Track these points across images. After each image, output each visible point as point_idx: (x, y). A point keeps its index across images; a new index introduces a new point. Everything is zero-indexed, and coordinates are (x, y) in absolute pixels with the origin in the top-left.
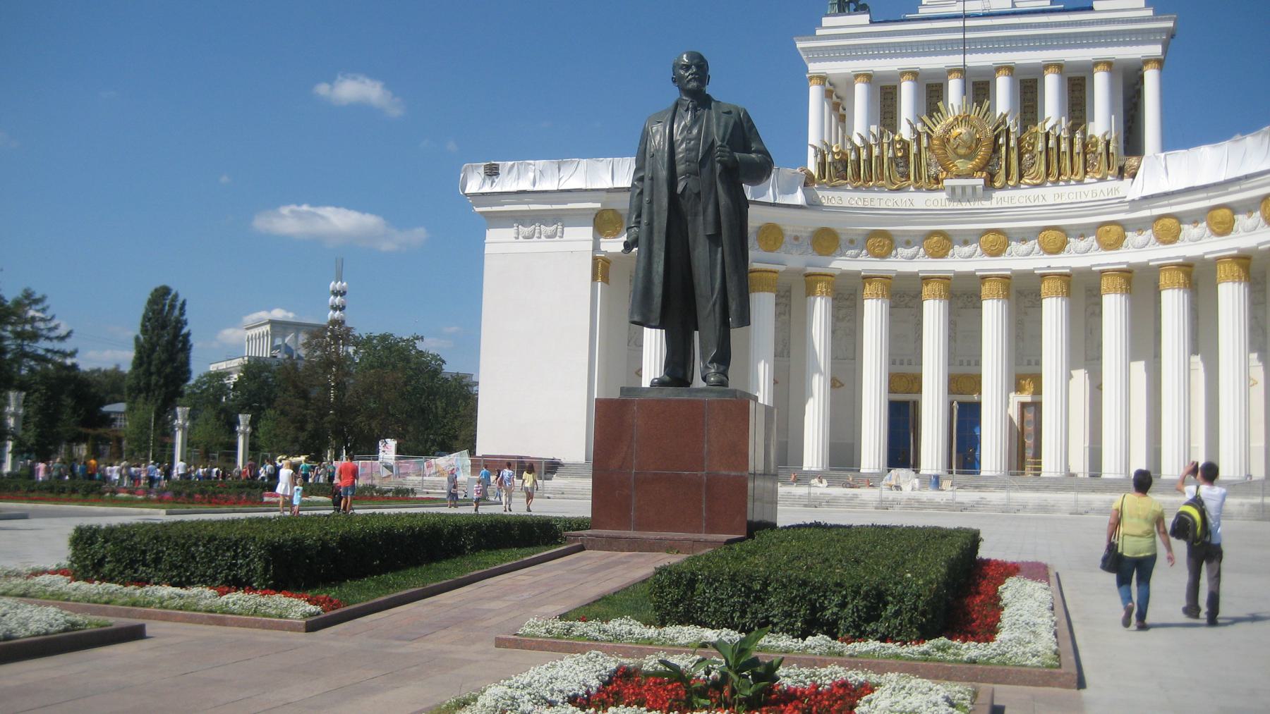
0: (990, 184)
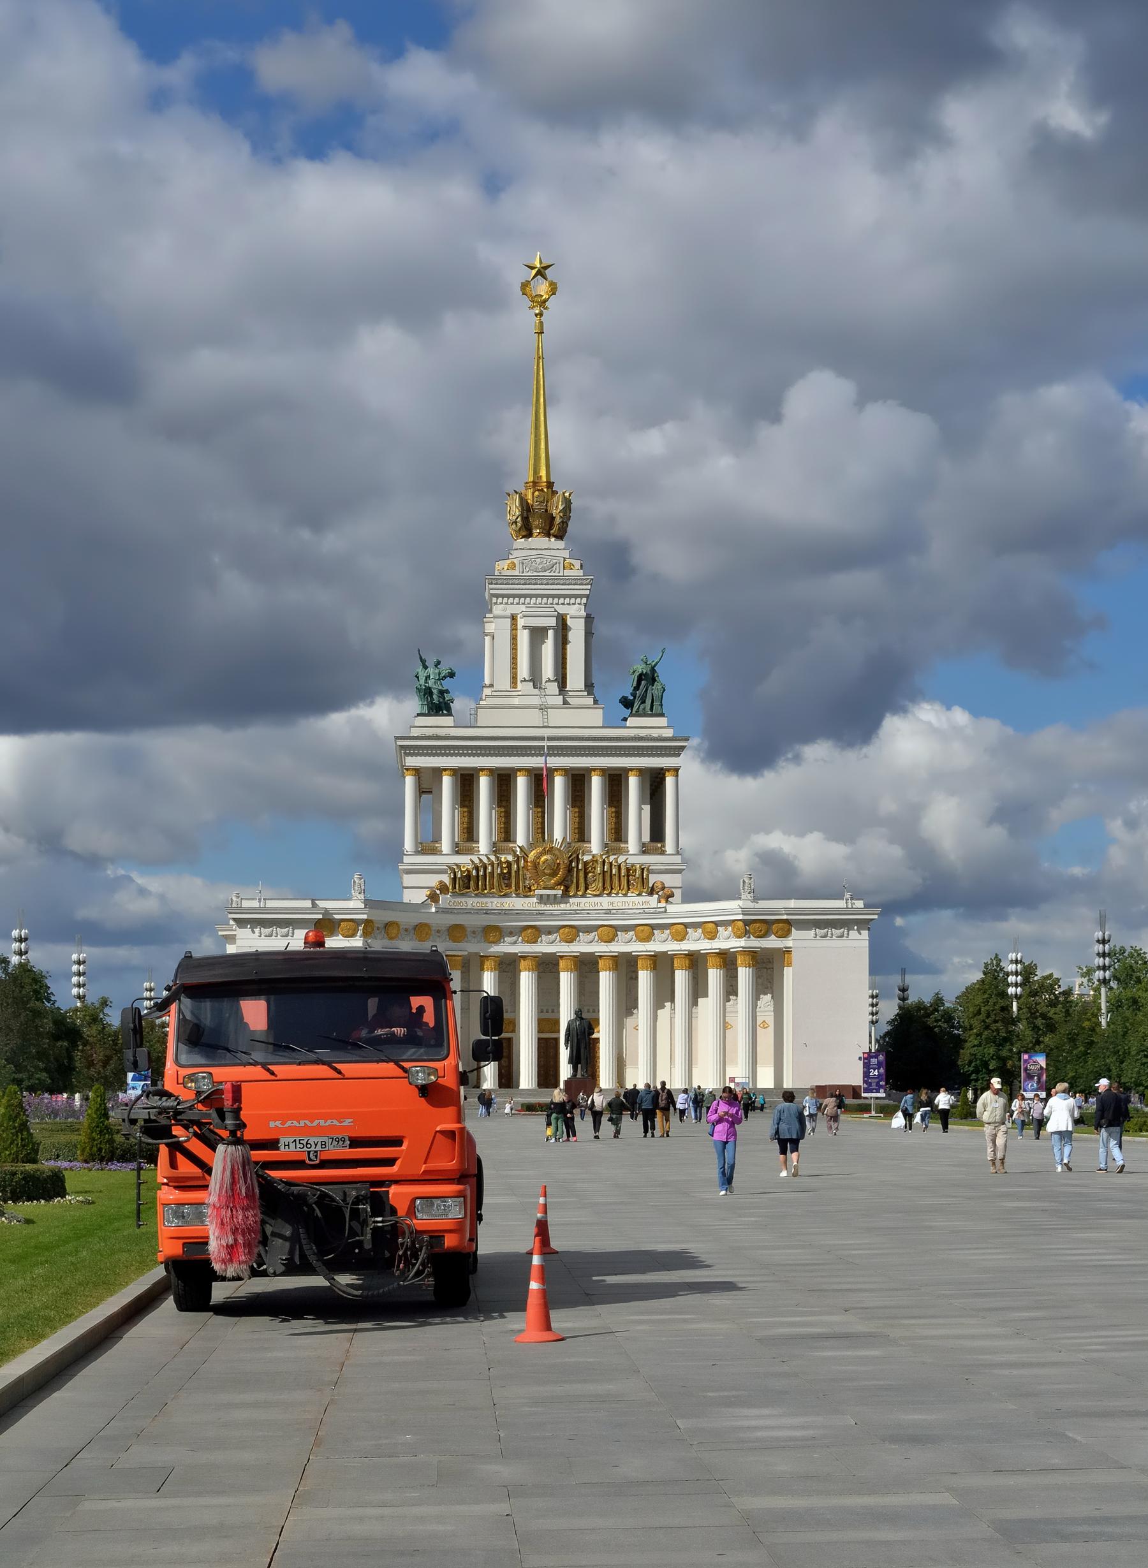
0: (566, 894)
